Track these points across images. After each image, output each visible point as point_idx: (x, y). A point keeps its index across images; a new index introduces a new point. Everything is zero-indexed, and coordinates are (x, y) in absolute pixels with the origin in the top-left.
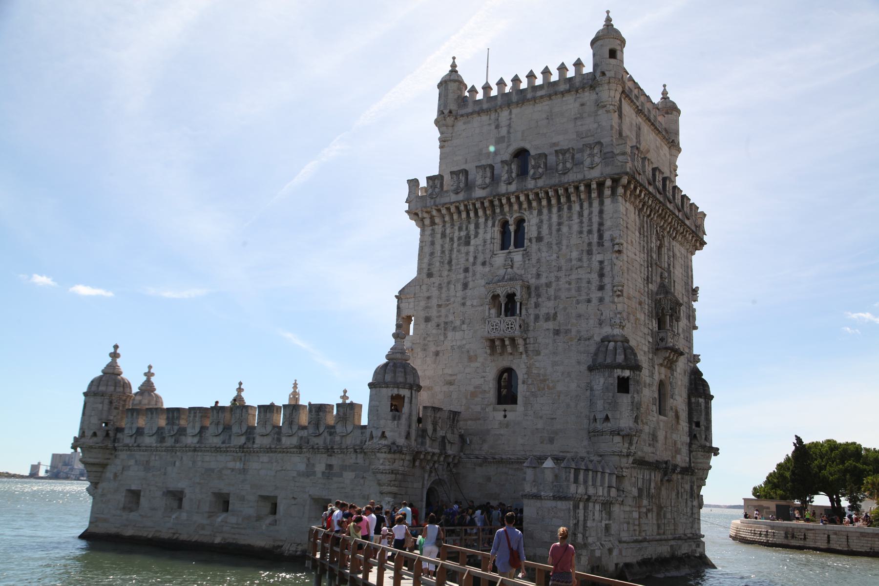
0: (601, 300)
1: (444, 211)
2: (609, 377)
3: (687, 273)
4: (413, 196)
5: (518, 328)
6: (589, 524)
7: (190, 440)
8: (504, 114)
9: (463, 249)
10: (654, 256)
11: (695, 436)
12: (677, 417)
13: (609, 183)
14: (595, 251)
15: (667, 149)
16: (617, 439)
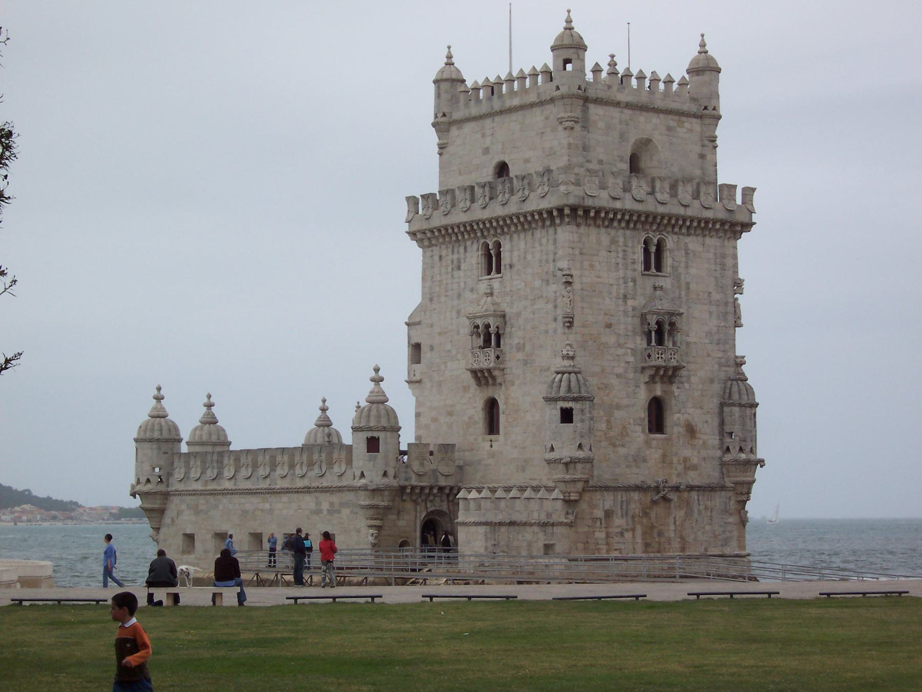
0: (555, 331)
1: (436, 233)
2: (555, 408)
3: (723, 265)
4: (411, 215)
5: (493, 357)
6: (515, 544)
7: (228, 485)
8: (488, 122)
9: (456, 273)
10: (640, 267)
11: (728, 449)
12: (691, 431)
13: (555, 213)
14: (551, 281)
15: (694, 120)
16: (561, 467)
